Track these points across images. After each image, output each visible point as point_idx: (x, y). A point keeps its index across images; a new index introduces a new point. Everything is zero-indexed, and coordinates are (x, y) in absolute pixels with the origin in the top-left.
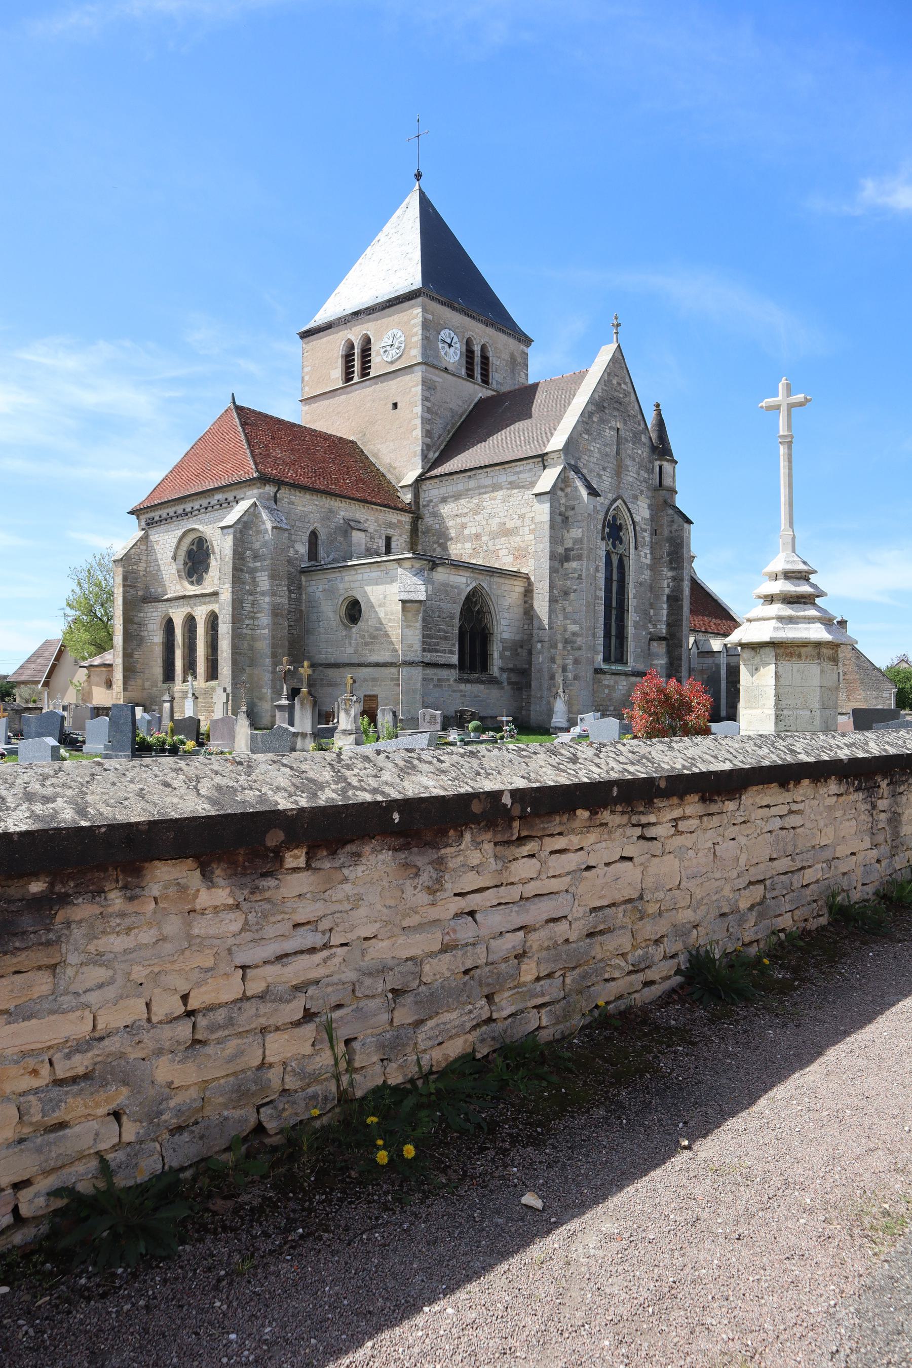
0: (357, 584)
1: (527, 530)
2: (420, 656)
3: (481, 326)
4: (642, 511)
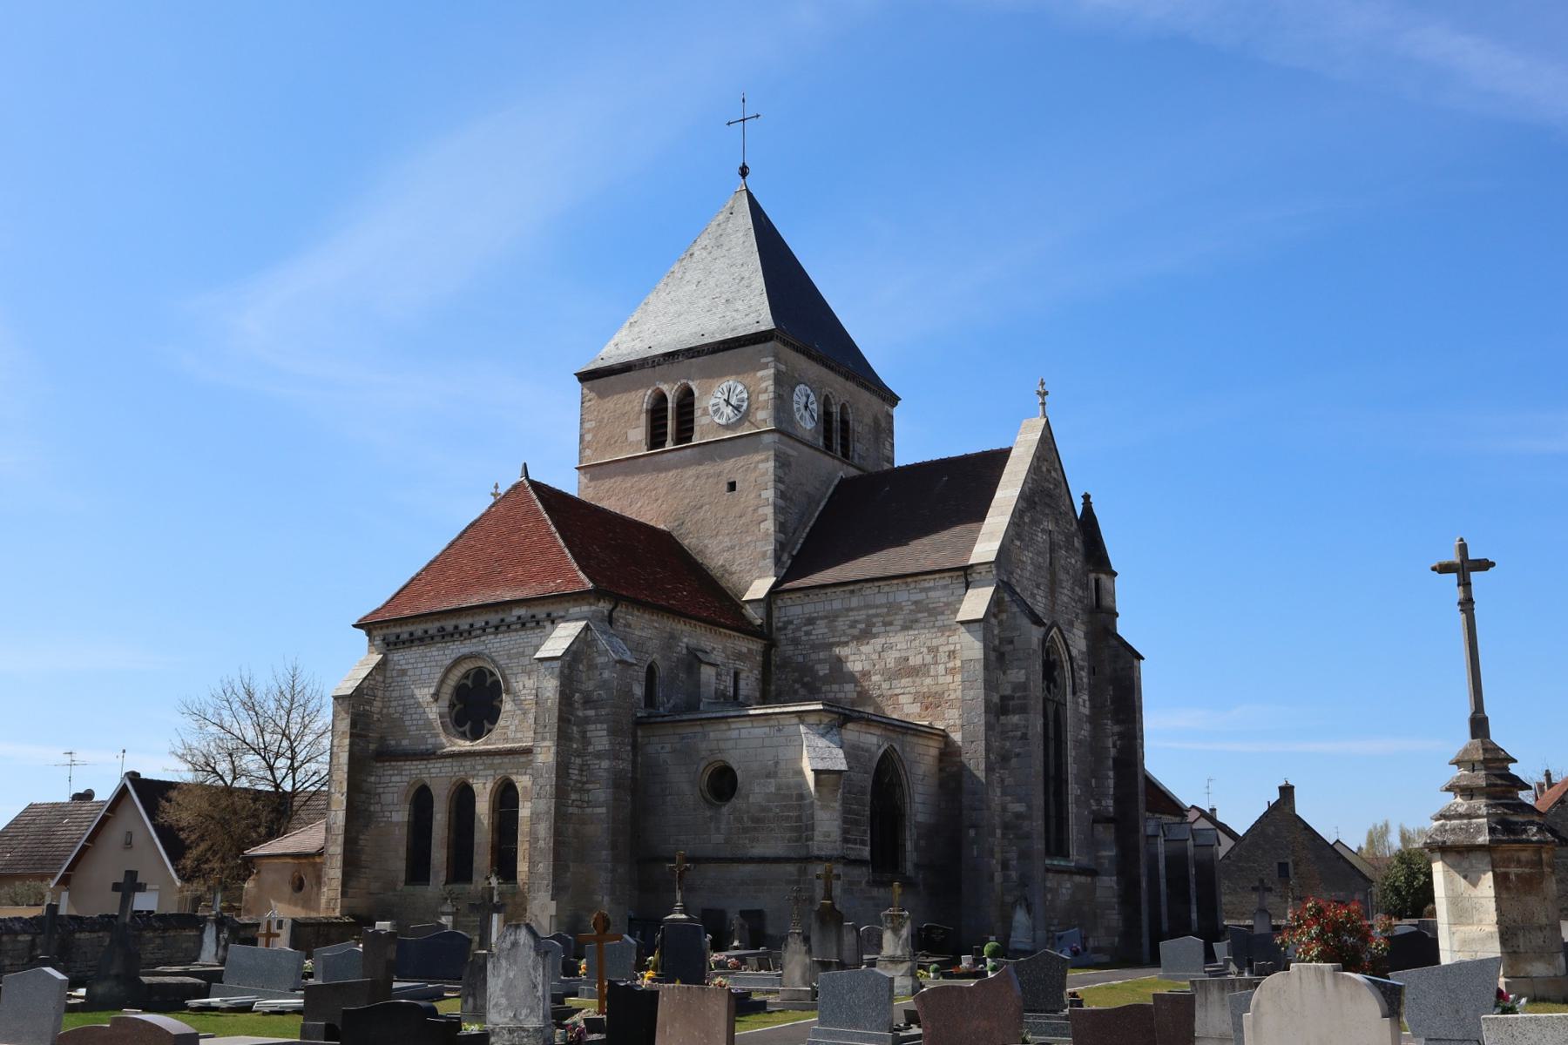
0: (730, 744)
1: (941, 669)
3: (841, 380)
4: (1078, 642)
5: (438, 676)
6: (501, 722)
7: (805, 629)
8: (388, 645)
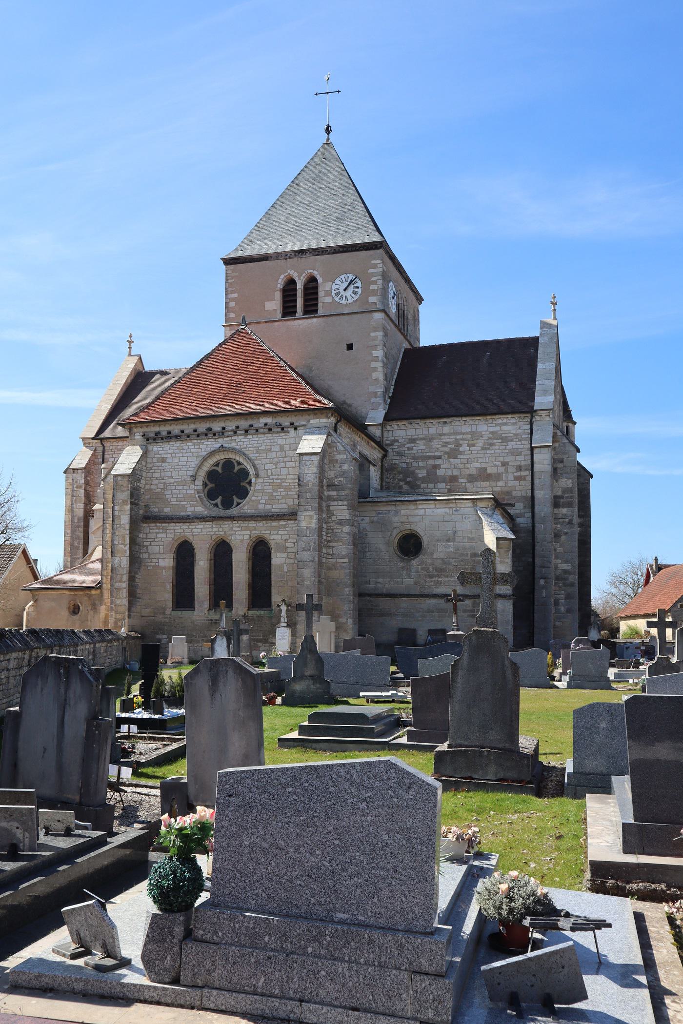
1: (511, 477)
7: (407, 446)
8: (148, 440)
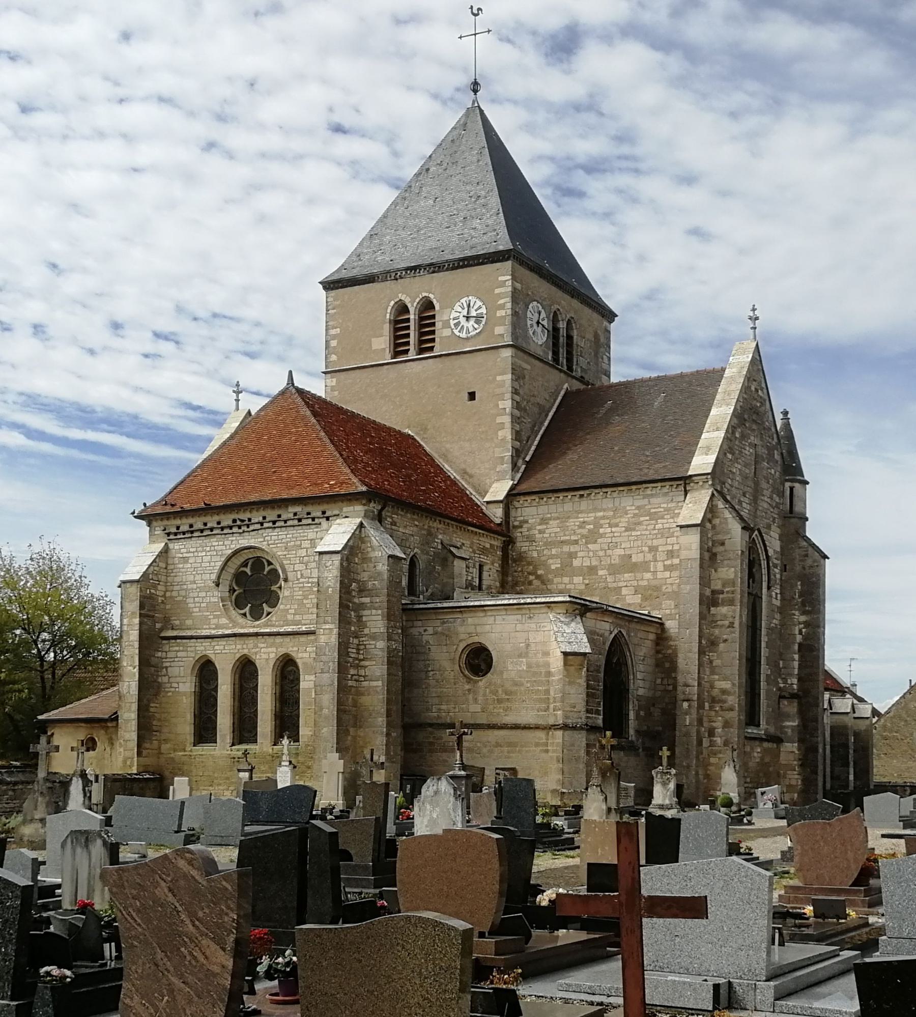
1: (660, 566)
2: (584, 717)
4: (774, 544)
5: (219, 564)
6: (281, 606)
